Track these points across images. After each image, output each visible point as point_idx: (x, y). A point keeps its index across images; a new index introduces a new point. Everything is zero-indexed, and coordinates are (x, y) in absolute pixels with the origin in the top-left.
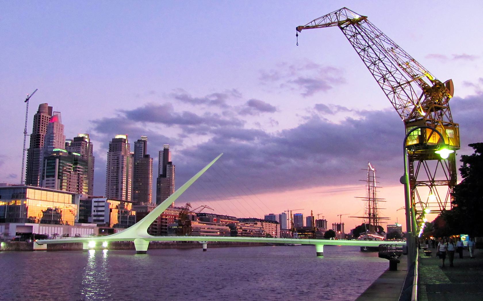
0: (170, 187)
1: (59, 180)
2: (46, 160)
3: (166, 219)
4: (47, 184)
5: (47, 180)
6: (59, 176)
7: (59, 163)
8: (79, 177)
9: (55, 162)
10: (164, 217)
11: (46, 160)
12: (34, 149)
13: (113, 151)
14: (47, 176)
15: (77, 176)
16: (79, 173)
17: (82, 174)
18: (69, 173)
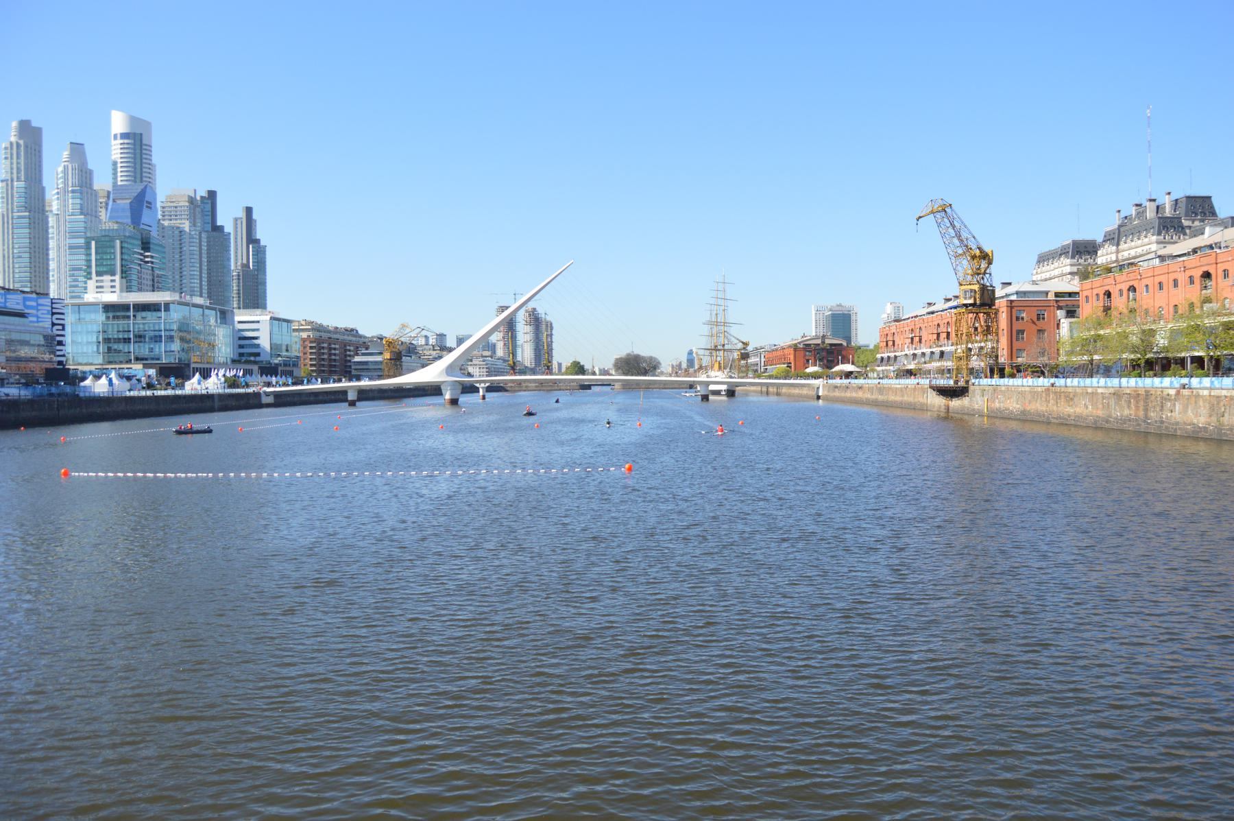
0: (260, 287)
1: (124, 280)
2: (93, 243)
3: (335, 349)
4: (97, 287)
5: (97, 281)
6: (122, 272)
7: (122, 248)
8: (153, 275)
9: (114, 247)
10: (333, 346)
11: (93, 243)
12: (15, 214)
13: (171, 220)
14: (99, 274)
15: (150, 272)
16: (152, 268)
17: (160, 269)
18: (139, 268)
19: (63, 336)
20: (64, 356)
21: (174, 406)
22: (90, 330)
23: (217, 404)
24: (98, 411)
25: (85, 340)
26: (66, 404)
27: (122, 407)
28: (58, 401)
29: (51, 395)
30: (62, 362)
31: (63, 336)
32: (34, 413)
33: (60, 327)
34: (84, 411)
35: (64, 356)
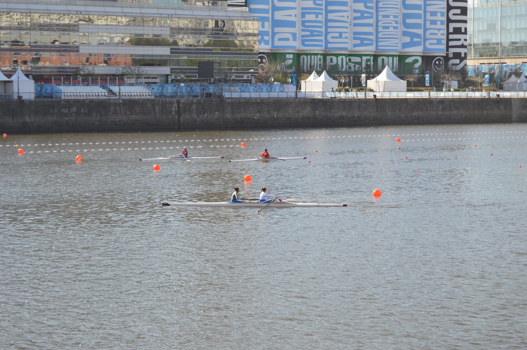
19: (465, 22)
20: (463, 46)
21: (415, 114)
22: (519, 14)
23: (515, 112)
24: (257, 116)
25: (514, 27)
26: (194, 107)
27: (306, 112)
28: (178, 102)
29: (209, 95)
30: (460, 53)
31: (465, 22)
32: (134, 117)
33: (458, 11)
34: (229, 116)
35: (463, 46)
